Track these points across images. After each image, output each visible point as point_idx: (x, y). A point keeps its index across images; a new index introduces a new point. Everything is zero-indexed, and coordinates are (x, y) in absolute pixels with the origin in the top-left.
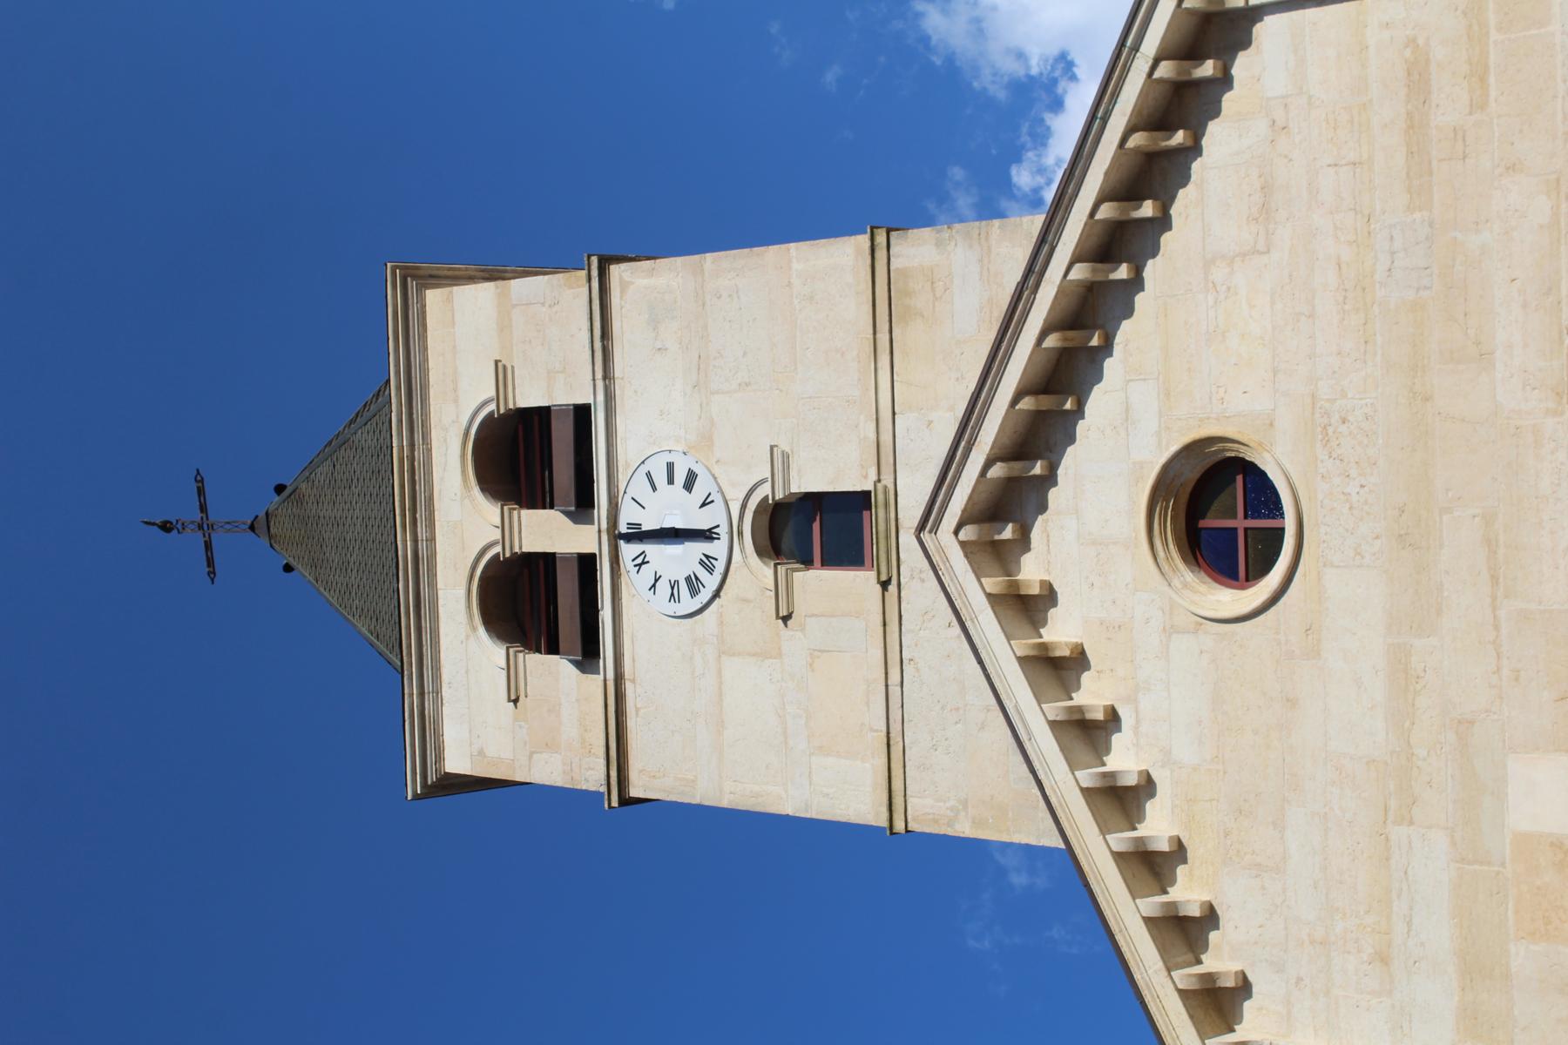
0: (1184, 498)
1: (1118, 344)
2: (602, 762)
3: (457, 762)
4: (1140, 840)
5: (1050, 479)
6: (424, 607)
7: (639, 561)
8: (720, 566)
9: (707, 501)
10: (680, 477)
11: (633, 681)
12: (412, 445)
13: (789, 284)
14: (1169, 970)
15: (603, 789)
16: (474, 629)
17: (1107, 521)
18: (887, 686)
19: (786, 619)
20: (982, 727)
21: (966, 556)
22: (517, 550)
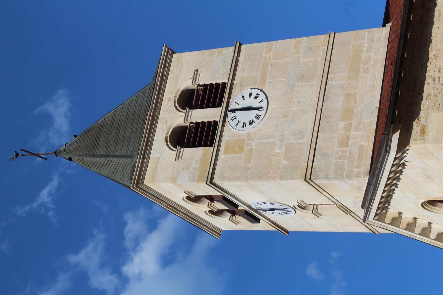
12: (166, 203)
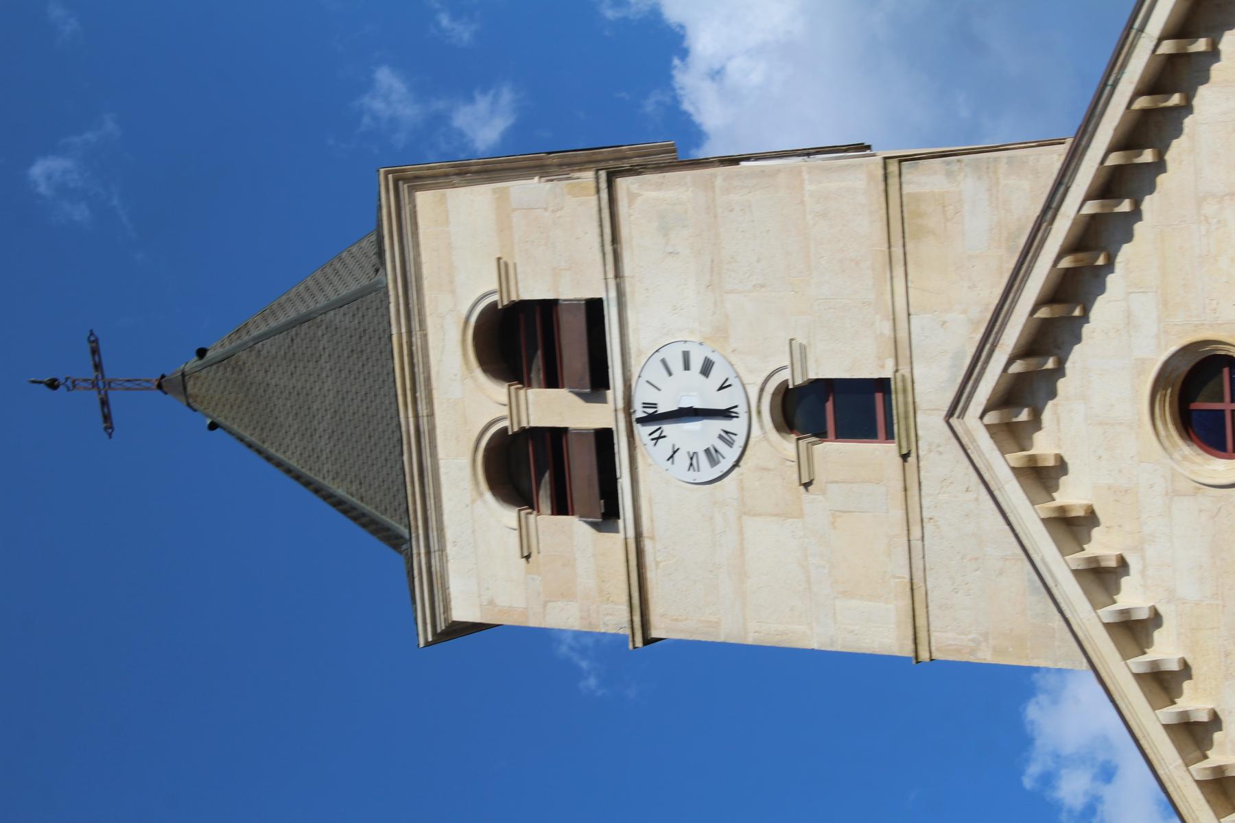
1: (1120, 263)
2: (624, 608)
3: (462, 612)
4: (1154, 663)
5: (1059, 371)
6: (427, 475)
7: (656, 435)
8: (739, 441)
10: (697, 364)
11: (652, 538)
12: (410, 332)
13: (802, 202)
15: (628, 632)
16: (481, 494)
17: (1112, 406)
18: (909, 541)
19: (806, 485)
20: (1001, 573)
21: (992, 437)
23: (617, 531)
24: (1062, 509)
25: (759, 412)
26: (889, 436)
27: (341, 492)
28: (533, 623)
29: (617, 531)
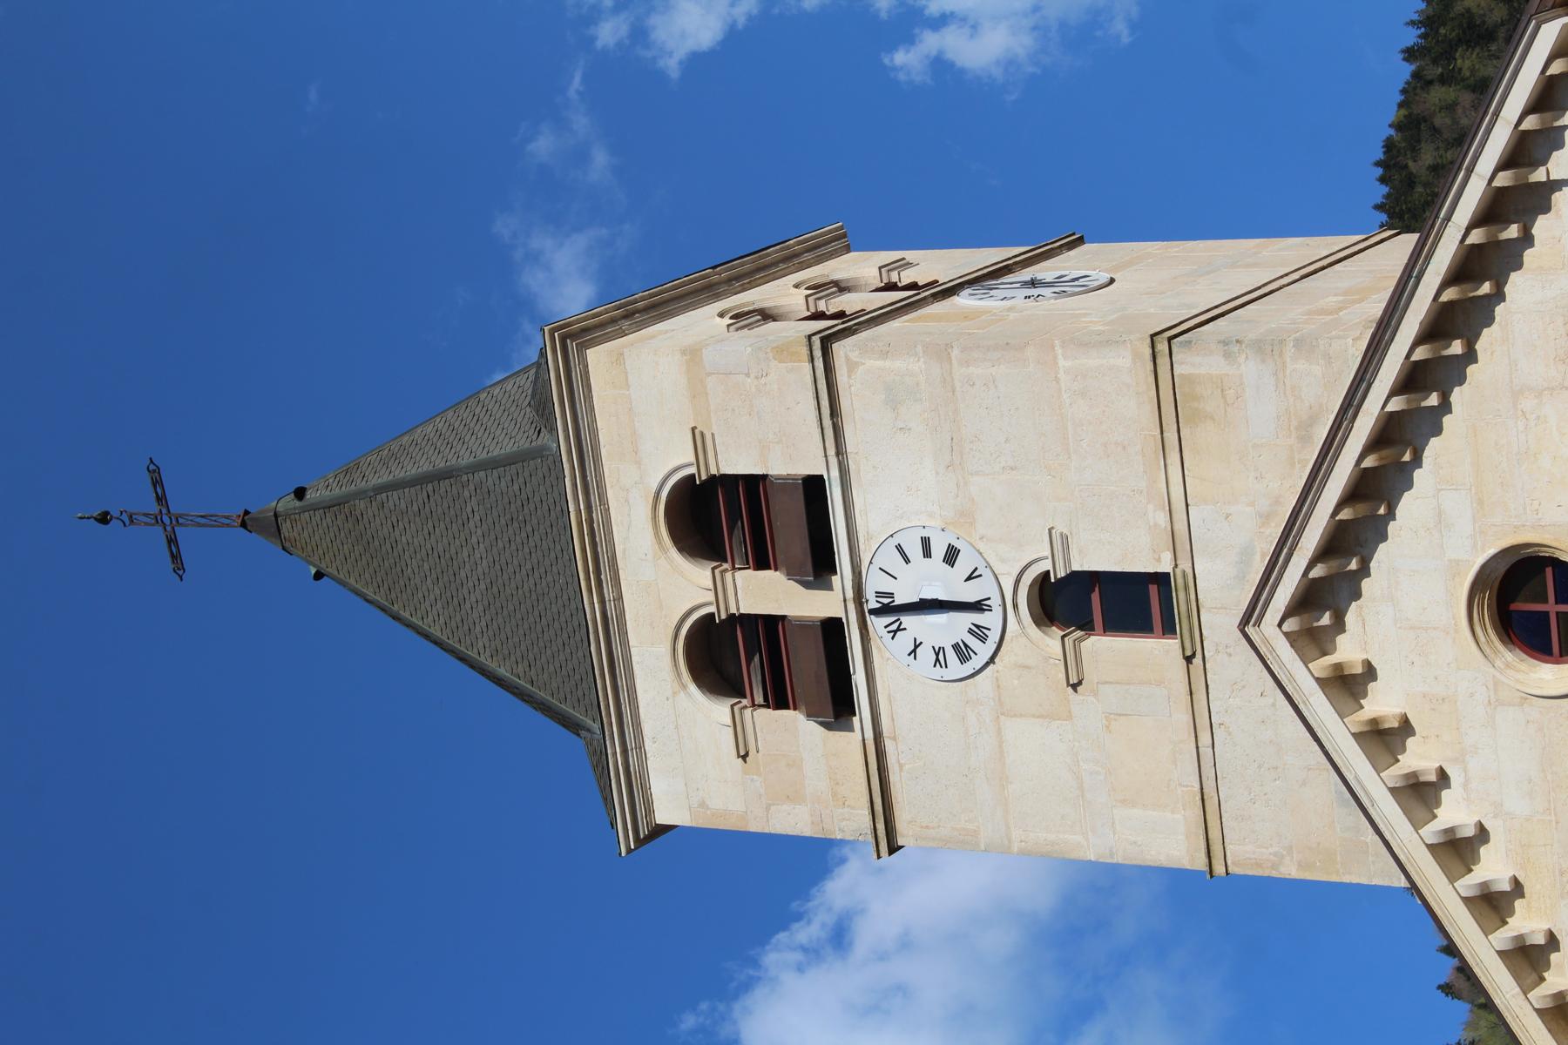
0: (1496, 585)
1: (1426, 458)
2: (866, 812)
4: (1485, 885)
5: (1364, 571)
6: (618, 666)
7: (894, 627)
8: (994, 637)
9: (974, 575)
10: (939, 551)
11: (894, 739)
13: (1057, 380)
14: (1525, 994)
15: (871, 839)
16: (684, 687)
17: (1425, 609)
18: (1197, 748)
19: (1075, 687)
20: (1304, 783)
22: (733, 610)
23: (851, 729)
24: (1374, 722)
25: (1015, 606)
26: (1169, 629)
27: (502, 671)
28: (754, 827)
29: (851, 729)
